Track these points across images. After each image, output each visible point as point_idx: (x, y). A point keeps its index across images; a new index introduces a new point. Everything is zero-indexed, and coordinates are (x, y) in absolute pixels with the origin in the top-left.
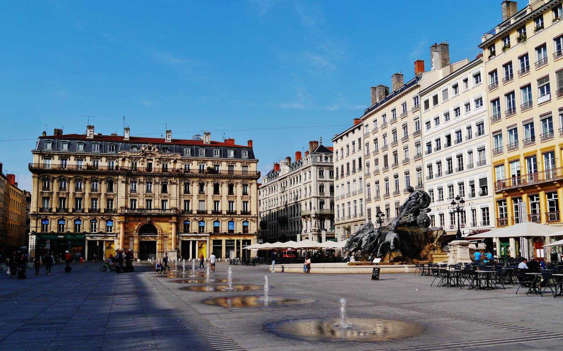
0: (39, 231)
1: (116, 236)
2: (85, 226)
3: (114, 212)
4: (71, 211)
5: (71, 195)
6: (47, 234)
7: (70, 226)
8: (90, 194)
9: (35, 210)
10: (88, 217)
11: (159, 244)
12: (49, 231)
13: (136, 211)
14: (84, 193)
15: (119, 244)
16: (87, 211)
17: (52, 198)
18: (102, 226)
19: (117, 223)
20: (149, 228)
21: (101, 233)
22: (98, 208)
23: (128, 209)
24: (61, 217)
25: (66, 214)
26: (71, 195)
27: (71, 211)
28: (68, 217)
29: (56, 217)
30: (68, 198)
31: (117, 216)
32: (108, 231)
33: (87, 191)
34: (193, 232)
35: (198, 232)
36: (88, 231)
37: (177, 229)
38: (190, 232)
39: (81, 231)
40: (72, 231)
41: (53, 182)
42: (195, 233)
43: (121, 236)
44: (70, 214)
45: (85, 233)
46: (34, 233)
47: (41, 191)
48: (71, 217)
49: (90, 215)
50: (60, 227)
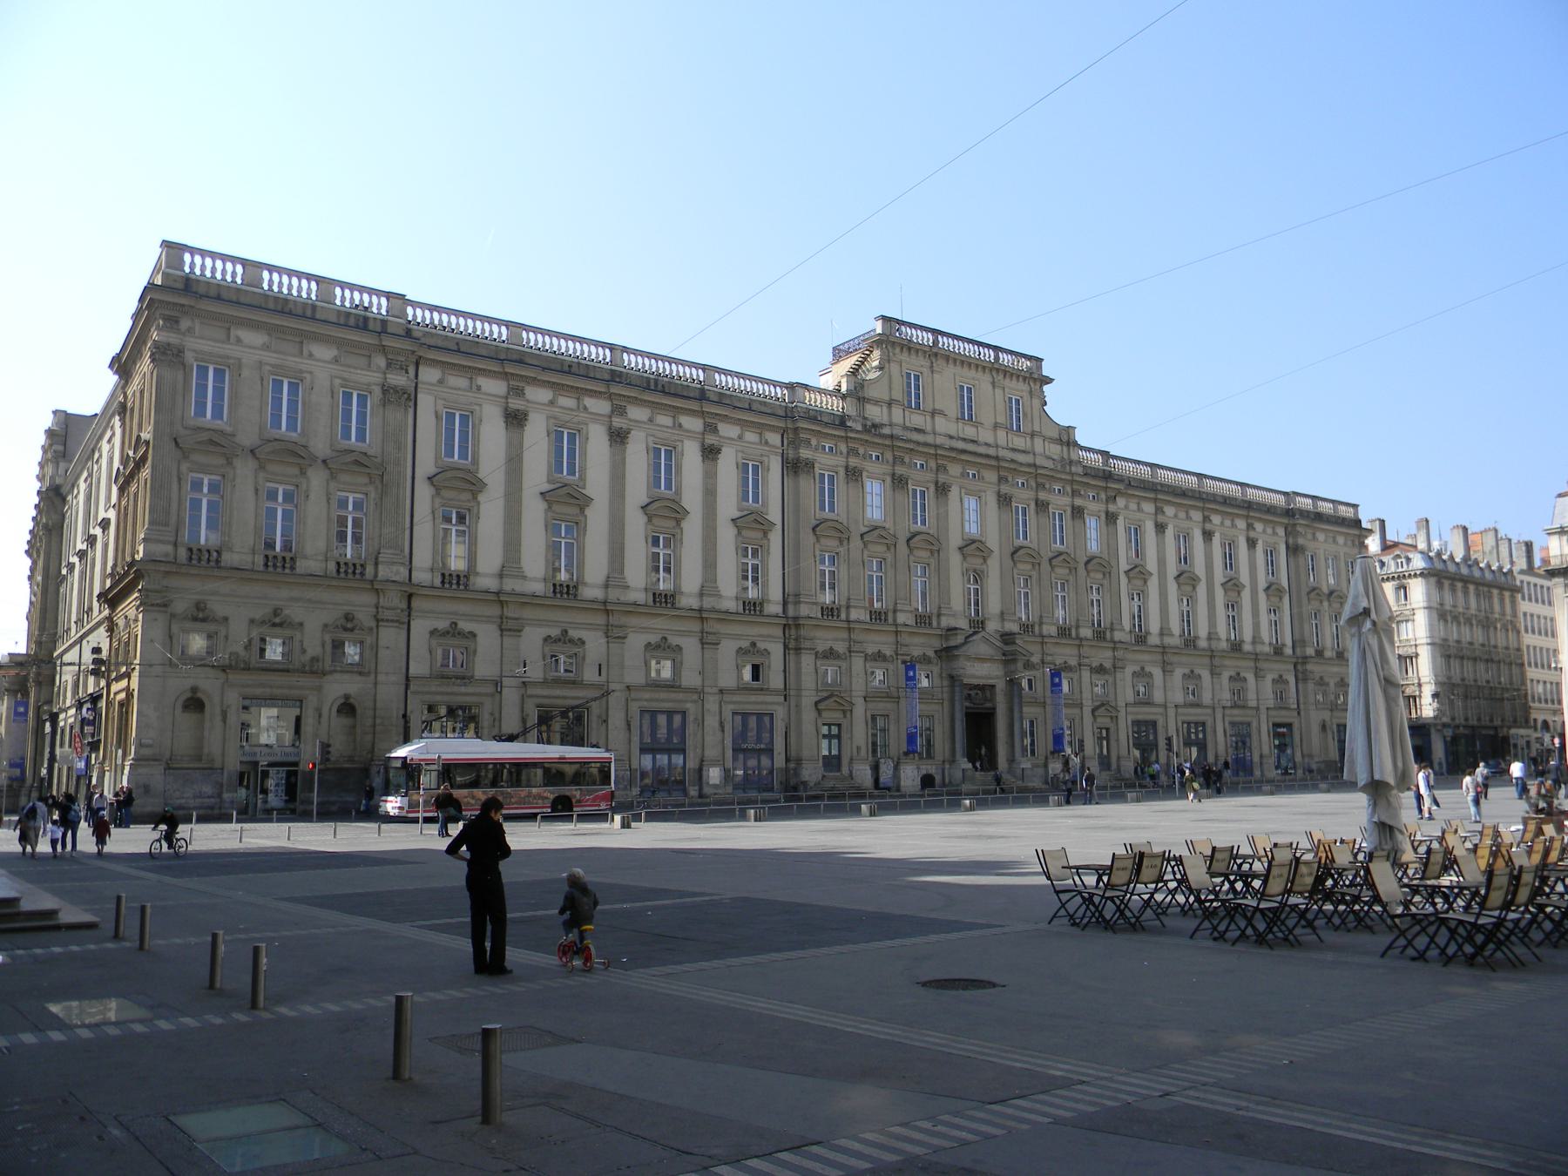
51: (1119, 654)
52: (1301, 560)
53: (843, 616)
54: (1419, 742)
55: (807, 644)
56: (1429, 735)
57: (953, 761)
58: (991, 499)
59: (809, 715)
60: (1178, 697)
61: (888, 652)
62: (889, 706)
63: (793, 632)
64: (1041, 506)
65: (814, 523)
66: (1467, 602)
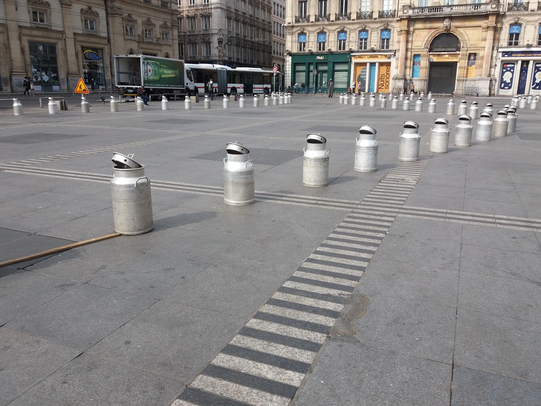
0: (295, 50)
1: (395, 55)
3: (393, 16)
4: (333, 18)
6: (304, 55)
9: (290, 21)
10: (357, 26)
11: (460, 68)
12: (307, 51)
13: (426, 12)
15: (397, 68)
18: (374, 40)
19: (396, 33)
20: (446, 40)
21: (373, 51)
23: (414, 9)
24: (322, 28)
25: (327, 23)
27: (333, 18)
28: (330, 28)
29: (316, 28)
31: (398, 21)
32: (383, 47)
34: (525, 44)
35: (535, 43)
36: (355, 47)
37: (496, 39)
38: (520, 44)
39: (347, 49)
40: (334, 49)
42: (529, 46)
43: (401, 54)
45: (351, 51)
46: (290, 54)
49: (358, 23)
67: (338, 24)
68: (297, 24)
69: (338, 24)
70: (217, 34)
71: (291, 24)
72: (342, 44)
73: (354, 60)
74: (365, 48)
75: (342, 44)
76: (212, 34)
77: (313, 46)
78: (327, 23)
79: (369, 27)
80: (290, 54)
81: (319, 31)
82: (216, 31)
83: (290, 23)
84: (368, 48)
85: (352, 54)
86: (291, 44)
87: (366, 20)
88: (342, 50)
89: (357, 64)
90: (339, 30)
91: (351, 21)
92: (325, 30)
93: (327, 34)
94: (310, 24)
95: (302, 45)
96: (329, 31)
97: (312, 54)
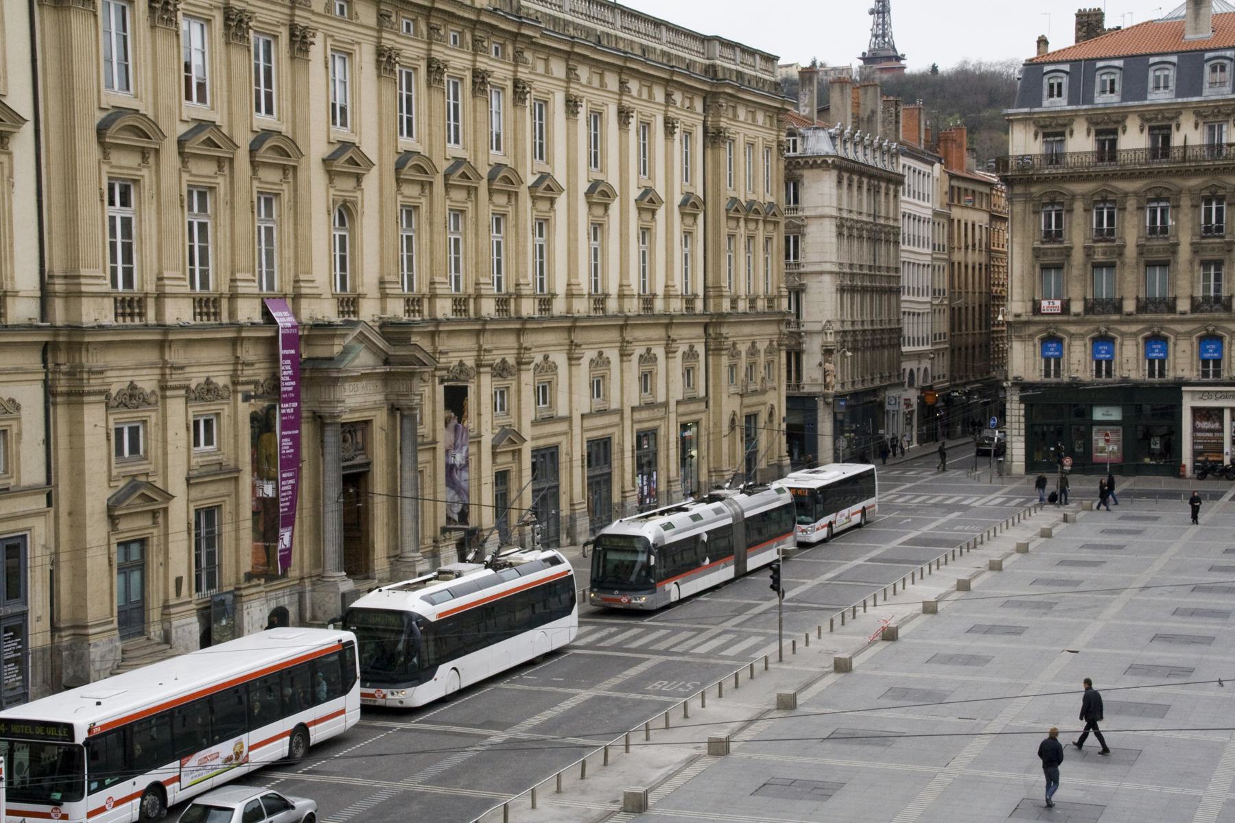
2: (1182, 361)
5: (1131, 252)
6: (1058, 386)
7: (1130, 363)
8: (1196, 249)
12: (1065, 378)
14: (1177, 245)
16: (1183, 305)
17: (1070, 266)
22: (1224, 293)
26: (1131, 252)
28: (1124, 328)
29: (1085, 328)
30: (1123, 264)
33: (1185, 240)
39: (1170, 375)
40: (1134, 376)
41: (1070, 211)
44: (1129, 319)
47: (1037, 244)
48: (1134, 328)
50: (1103, 366)
51: (528, 340)
52: (724, 154)
53: (151, 317)
54: (797, 420)
55: (94, 383)
56: (814, 411)
57: (319, 578)
58: (366, 56)
59: (96, 531)
60: (584, 402)
61: (222, 380)
62: (223, 489)
63: (62, 358)
64: (435, 69)
65: (99, 116)
66: (860, 201)
67: (1143, 322)
68: (1037, 318)
69: (1143, 322)
70: (819, 333)
71: (1024, 318)
72: (1157, 365)
73: (1188, 403)
74: (1217, 373)
75: (1157, 365)
76: (806, 332)
77: (1081, 367)
78: (1116, 317)
79: (1223, 329)
80: (1022, 385)
81: (1096, 334)
82: (818, 327)
83: (1018, 316)
84: (1225, 375)
85: (1184, 388)
86: (1023, 361)
87: (1217, 315)
88: (1157, 379)
89: (1196, 411)
90: (1148, 333)
91: (1177, 316)
92: (1111, 334)
93: (1118, 341)
94: (1072, 318)
95: (1053, 363)
96: (1123, 334)
97: (1075, 386)
